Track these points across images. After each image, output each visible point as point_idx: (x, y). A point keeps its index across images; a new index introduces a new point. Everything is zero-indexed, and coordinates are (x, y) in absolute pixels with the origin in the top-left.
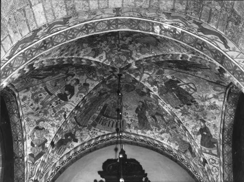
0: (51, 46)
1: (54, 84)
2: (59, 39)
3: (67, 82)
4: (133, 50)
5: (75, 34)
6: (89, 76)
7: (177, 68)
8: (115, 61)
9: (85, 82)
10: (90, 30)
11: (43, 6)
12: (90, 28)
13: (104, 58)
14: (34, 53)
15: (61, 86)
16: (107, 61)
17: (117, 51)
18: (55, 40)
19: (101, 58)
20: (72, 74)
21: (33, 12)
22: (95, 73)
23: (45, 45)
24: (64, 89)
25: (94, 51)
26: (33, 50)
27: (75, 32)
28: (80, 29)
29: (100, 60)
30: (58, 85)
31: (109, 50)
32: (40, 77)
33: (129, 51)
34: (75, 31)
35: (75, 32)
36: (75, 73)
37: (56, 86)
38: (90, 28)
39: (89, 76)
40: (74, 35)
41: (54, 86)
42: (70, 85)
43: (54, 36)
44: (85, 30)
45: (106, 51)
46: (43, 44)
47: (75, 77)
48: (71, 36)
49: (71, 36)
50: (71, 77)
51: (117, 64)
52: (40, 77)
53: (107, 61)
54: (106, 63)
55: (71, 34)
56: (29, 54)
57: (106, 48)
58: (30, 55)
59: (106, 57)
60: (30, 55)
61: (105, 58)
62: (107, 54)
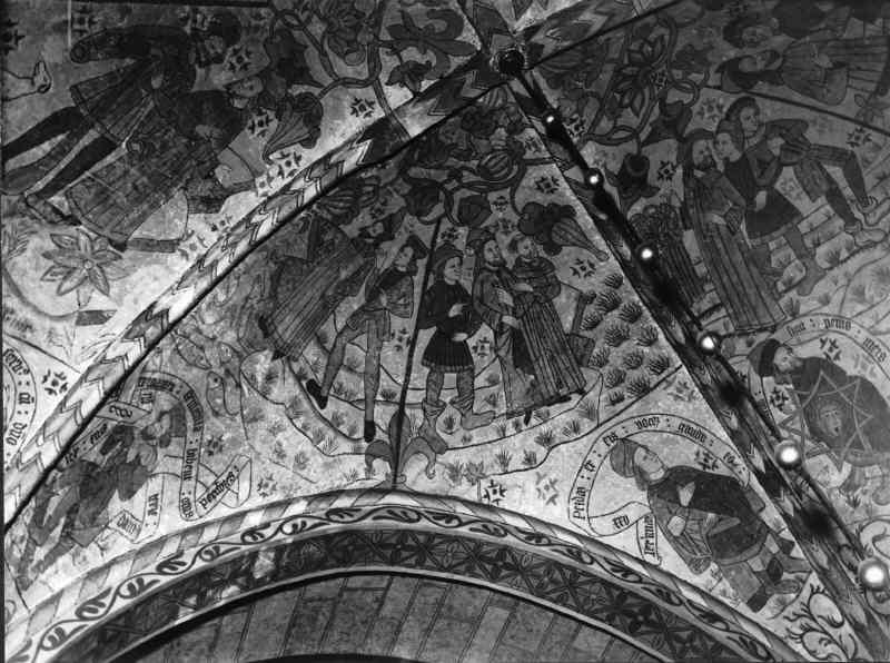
0: (630, 600)
1: (840, 76)
2: (594, 597)
3: (780, 51)
4: (391, 183)
5: (541, 571)
6: (667, 37)
7: (187, 29)
8: (496, 128)
9: (707, 13)
10: (494, 555)
11: (574, 638)
12: (490, 561)
13: (533, 174)
14: (684, 635)
15: (820, 49)
16: (529, 155)
17: (465, 173)
18: (607, 603)
19: (548, 186)
20: (729, 83)
21: (607, 649)
22: (626, 49)
23: (641, 618)
24: (822, 26)
25: (557, 240)
26: (678, 646)
27: (538, 577)
28: (519, 578)
29: (555, 181)
30: (825, 62)
31: (493, 197)
32: (842, 183)
33: (414, 172)
34: (535, 582)
35: (538, 577)
36: (714, 79)
37: (838, 65)
38: (490, 561)
39: (667, 37)
40: (548, 572)
41: (844, 69)
42: (782, 29)
43: (599, 615)
44: (507, 566)
45: (508, 197)
46: (643, 628)
47: (732, 53)
48: (557, 575)
49: (557, 575)
50: (746, 66)
51: (492, 111)
52: (842, 183)
53: (529, 155)
54: (538, 150)
55: (553, 581)
56: (695, 649)
57: (501, 215)
58: (697, 643)
59: (522, 174)
60: (697, 643)
61: (530, 170)
62: (514, 184)
